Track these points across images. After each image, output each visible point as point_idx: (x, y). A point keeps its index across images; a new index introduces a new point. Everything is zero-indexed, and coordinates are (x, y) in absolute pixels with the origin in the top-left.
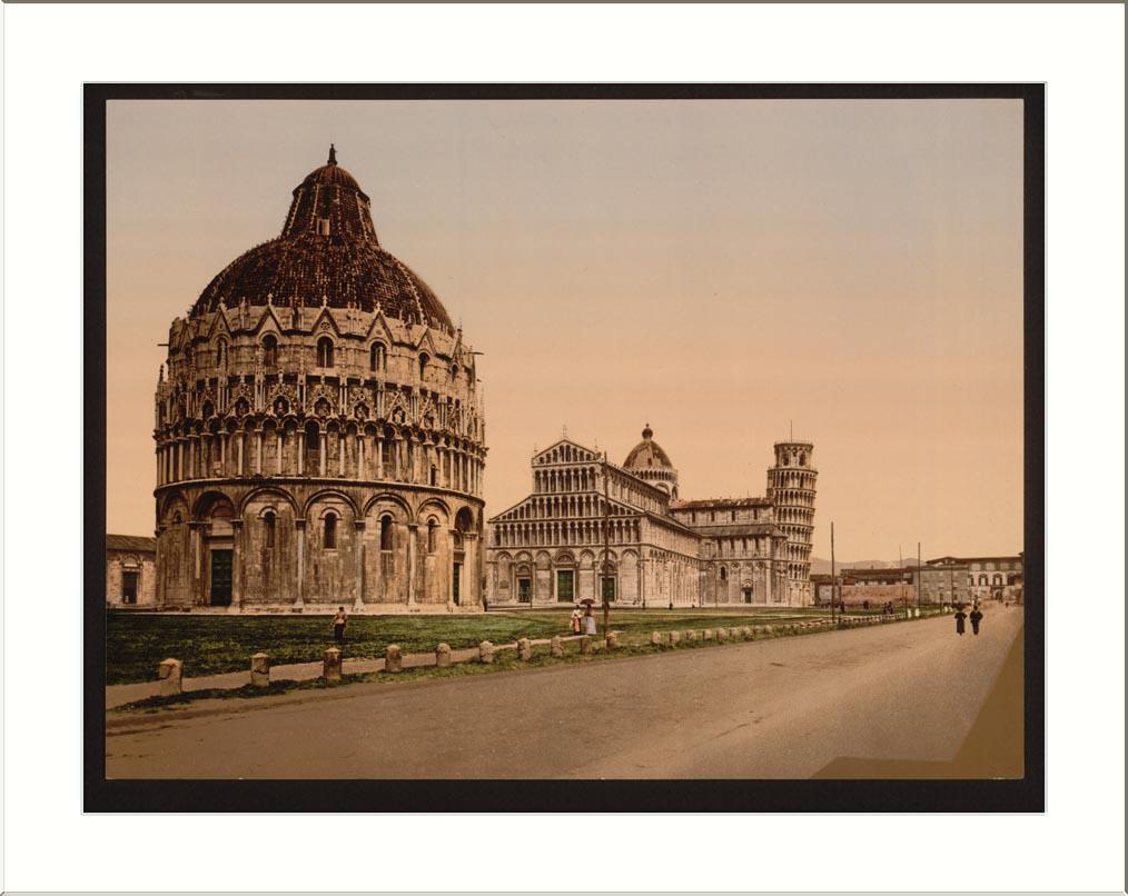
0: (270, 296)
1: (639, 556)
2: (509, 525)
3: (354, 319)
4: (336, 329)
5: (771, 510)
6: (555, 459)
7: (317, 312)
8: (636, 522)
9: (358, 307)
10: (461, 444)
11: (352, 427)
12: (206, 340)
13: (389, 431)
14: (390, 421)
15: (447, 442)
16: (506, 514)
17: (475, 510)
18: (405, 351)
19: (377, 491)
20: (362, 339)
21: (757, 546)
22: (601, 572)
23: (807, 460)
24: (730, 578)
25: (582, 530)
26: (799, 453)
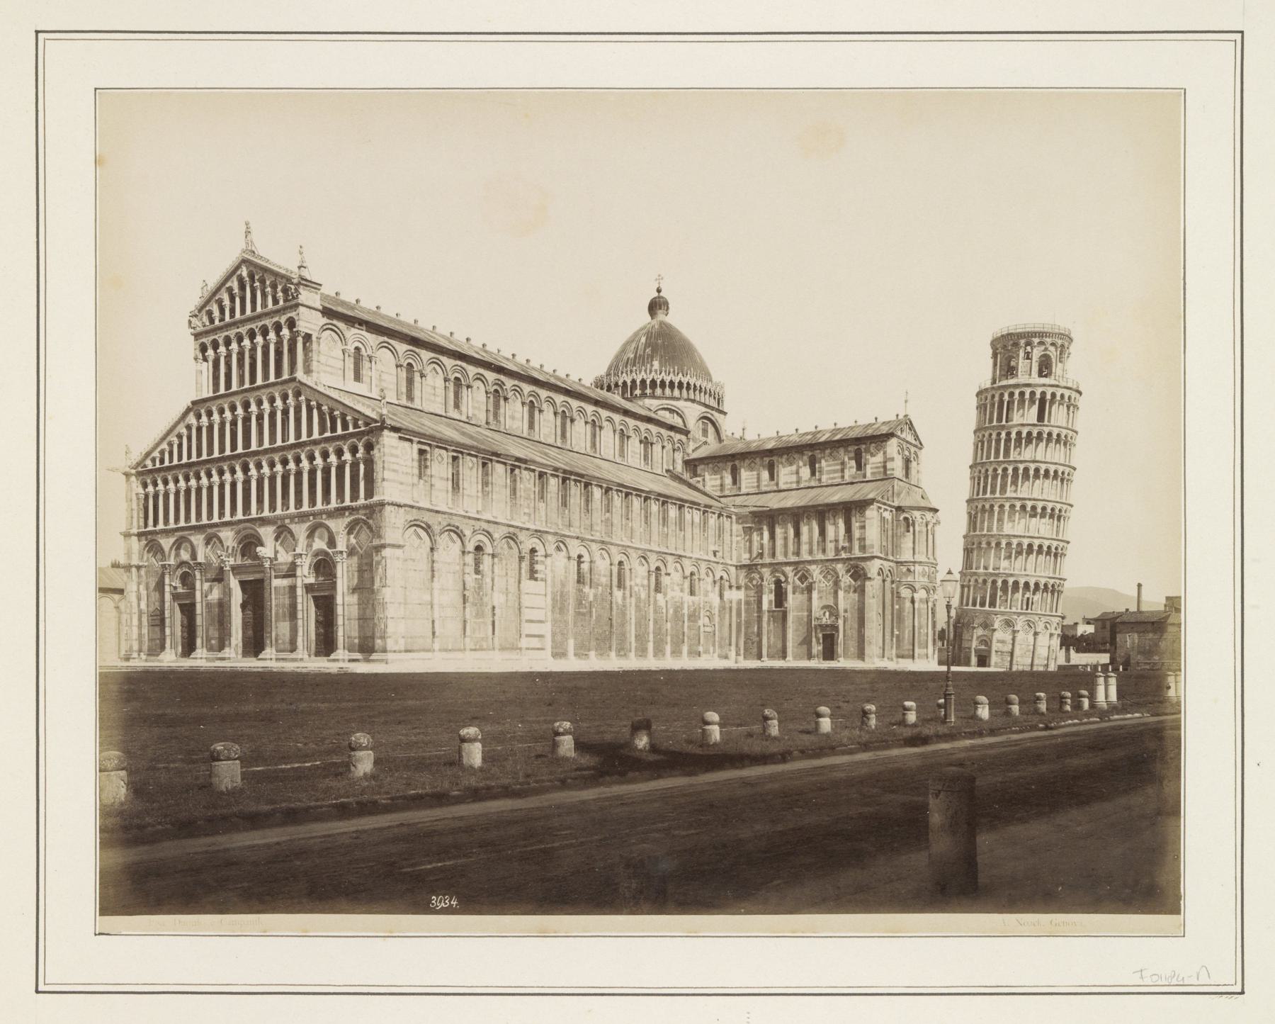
21: (849, 530)
23: (1057, 369)
24: (793, 601)
26: (1037, 353)
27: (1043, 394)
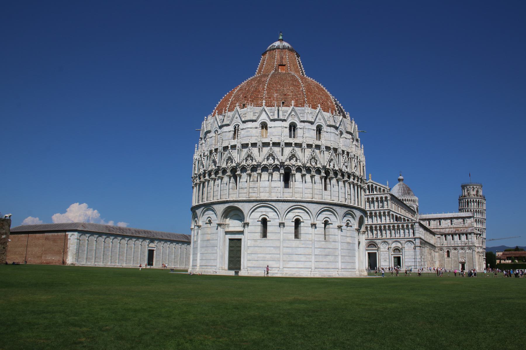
0: (264, 101)
3: (308, 112)
4: (299, 119)
5: (472, 219)
7: (289, 109)
8: (412, 226)
9: (309, 107)
10: (360, 181)
11: (308, 170)
12: (228, 125)
13: (327, 172)
14: (328, 167)
15: (354, 179)
18: (333, 130)
19: (323, 206)
20: (312, 123)
21: (467, 239)
22: (392, 253)
25: (382, 229)
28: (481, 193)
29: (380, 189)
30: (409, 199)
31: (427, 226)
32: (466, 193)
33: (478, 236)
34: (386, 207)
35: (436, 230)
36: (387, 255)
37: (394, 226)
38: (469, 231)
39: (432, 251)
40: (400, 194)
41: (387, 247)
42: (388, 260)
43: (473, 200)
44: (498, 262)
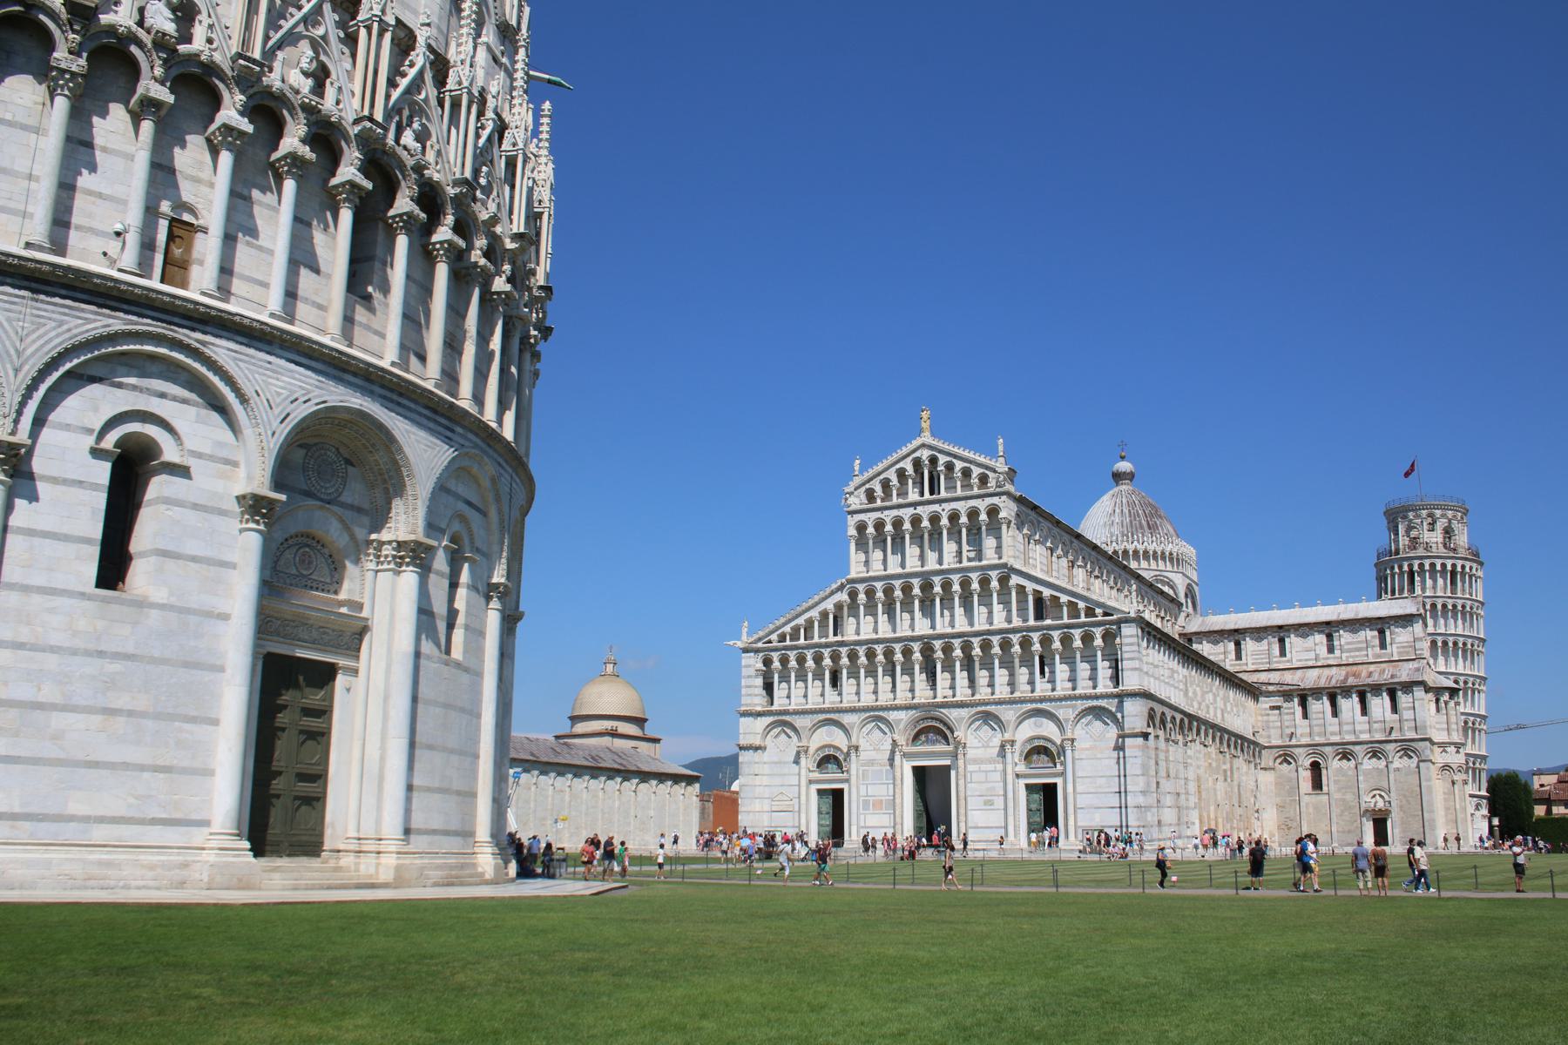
1: (1119, 724)
2: (792, 655)
6: (903, 493)
8: (1109, 637)
16: (787, 629)
17: (424, 454)
21: (1395, 709)
25: (973, 656)
26: (1440, 525)
27: (1454, 566)
28: (1462, 539)
29: (966, 473)
30: (1151, 548)
31: (1230, 664)
32: (1403, 541)
33: (1446, 697)
34: (990, 557)
35: (1263, 677)
36: (998, 776)
37: (1026, 643)
38: (1404, 678)
39: (1240, 763)
40: (1116, 530)
41: (997, 741)
42: (999, 803)
43: (1433, 565)
44: (1540, 811)
